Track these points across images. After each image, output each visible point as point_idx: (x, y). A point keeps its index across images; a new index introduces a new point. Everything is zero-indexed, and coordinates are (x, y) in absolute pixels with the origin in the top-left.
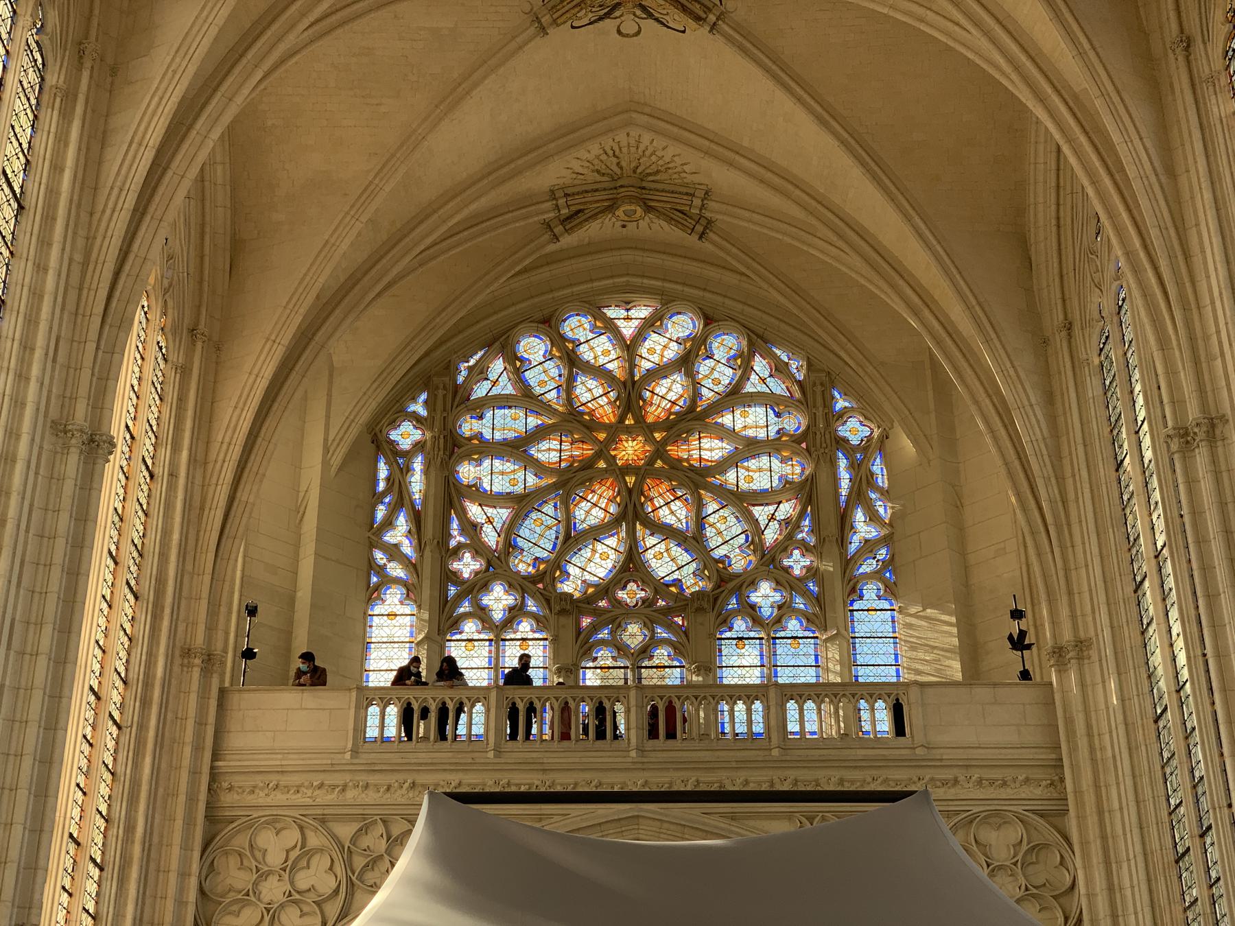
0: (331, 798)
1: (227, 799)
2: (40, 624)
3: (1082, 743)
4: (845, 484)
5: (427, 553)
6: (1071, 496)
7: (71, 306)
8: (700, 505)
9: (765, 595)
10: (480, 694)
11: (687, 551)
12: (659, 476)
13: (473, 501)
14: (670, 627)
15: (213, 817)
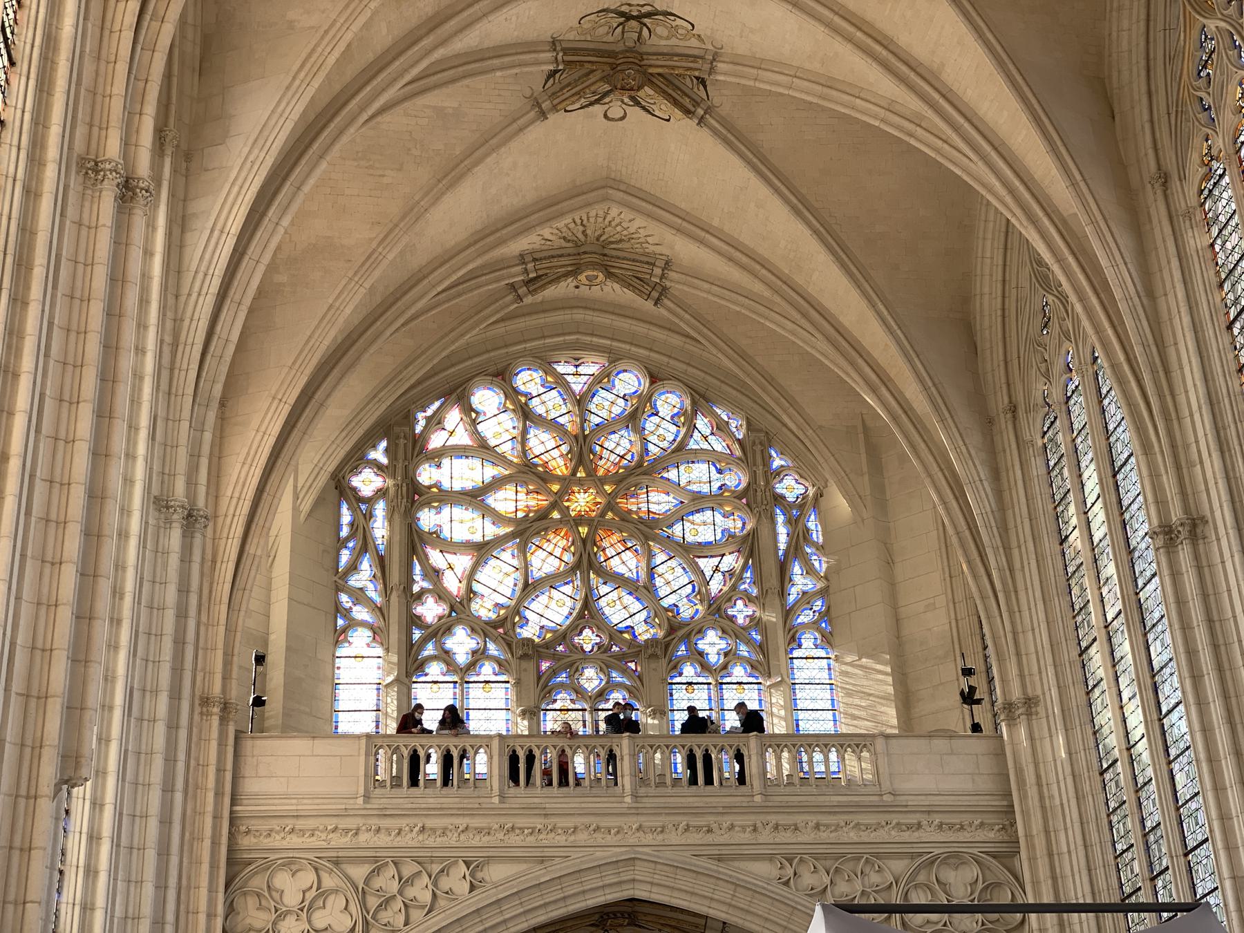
0: (345, 841)
1: (245, 842)
2: (156, 692)
3: (1032, 792)
4: (783, 539)
5: (394, 598)
6: (1017, 565)
7: (164, 386)
8: (650, 556)
9: (712, 644)
10: (485, 741)
11: (638, 599)
12: (610, 529)
13: (434, 548)
14: (625, 672)
15: (230, 862)
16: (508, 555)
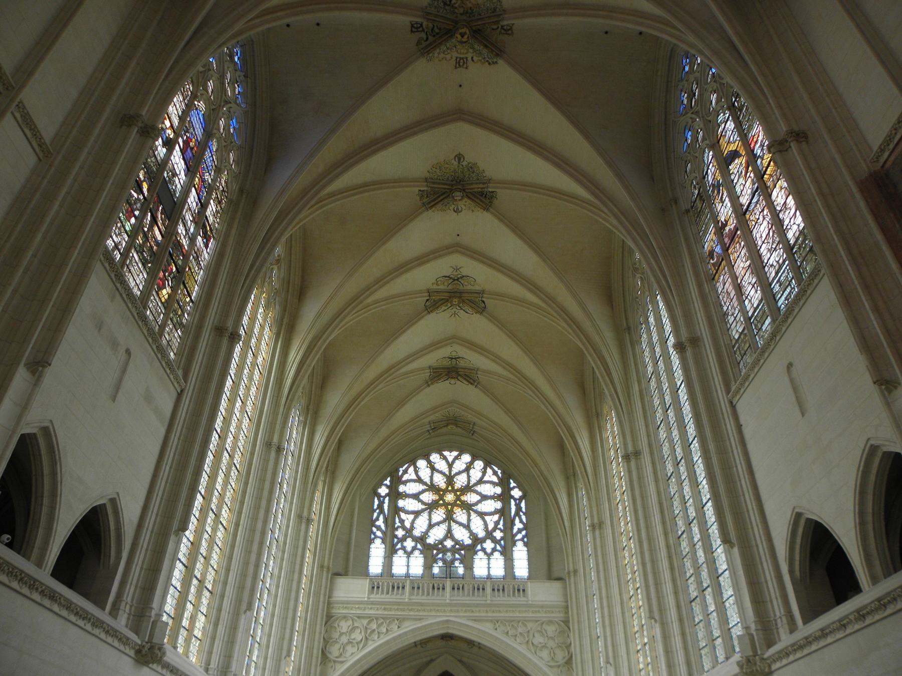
8: (469, 516)
9: (489, 545)
12: (458, 506)
16: (425, 515)
